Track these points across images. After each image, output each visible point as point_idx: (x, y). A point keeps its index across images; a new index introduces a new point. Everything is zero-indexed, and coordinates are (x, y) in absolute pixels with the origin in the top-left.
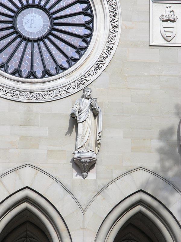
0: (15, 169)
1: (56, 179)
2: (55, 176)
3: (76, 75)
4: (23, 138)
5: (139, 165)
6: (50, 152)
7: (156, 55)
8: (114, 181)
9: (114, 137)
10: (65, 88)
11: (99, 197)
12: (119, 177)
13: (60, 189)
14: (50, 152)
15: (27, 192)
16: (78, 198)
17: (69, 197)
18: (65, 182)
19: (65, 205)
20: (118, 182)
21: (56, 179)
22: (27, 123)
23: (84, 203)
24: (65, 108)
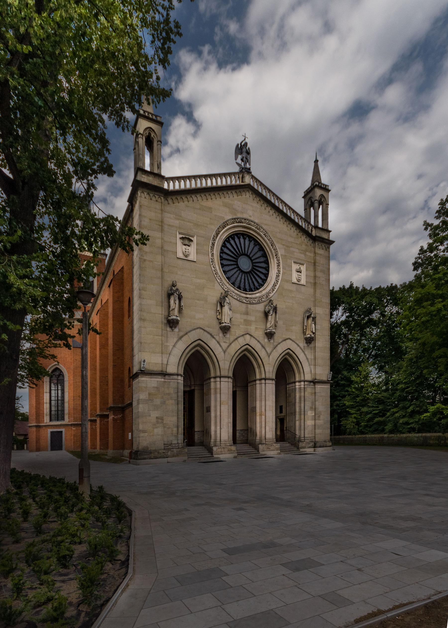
0: (243, 335)
1: (259, 341)
3: (264, 292)
4: (245, 320)
5: (288, 337)
7: (294, 288)
8: (279, 343)
9: (280, 323)
10: (261, 297)
11: (274, 351)
12: (281, 342)
13: (260, 346)
14: (256, 328)
15: (247, 346)
17: (263, 350)
18: (262, 342)
19: (263, 354)
20: (281, 344)
21: (259, 341)
22: (247, 313)
23: (269, 352)
24: (261, 307)
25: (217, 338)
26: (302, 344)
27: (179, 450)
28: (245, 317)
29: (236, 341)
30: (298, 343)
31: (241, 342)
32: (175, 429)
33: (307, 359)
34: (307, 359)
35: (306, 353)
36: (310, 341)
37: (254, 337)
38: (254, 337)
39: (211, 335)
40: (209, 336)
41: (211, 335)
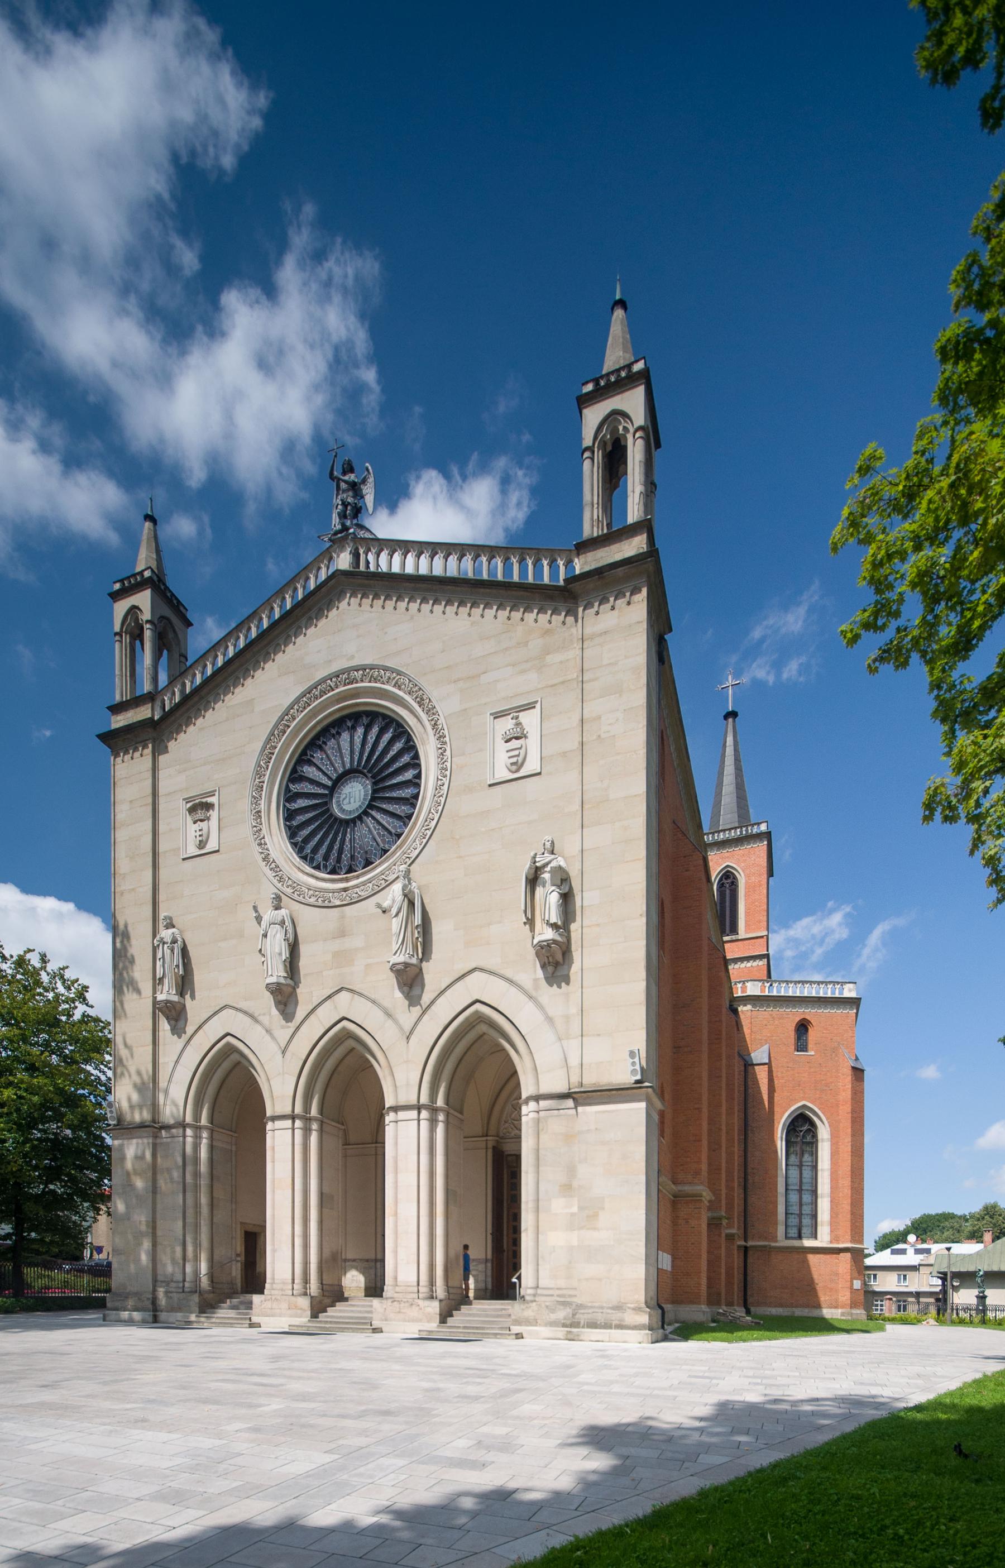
0: (329, 997)
1: (374, 1002)
2: (373, 997)
4: (336, 954)
5: (474, 966)
6: (368, 966)
13: (379, 1014)
14: (368, 966)
16: (401, 1021)
17: (390, 1022)
18: (386, 1003)
20: (447, 993)
25: (265, 1020)
26: (532, 973)
27: (182, 1295)
28: (336, 945)
29: (312, 1017)
30: (508, 973)
31: (326, 1016)
32: (179, 1250)
33: (550, 1020)
34: (550, 1020)
35: (544, 1000)
36: (556, 961)
37: (361, 994)
38: (361, 994)
39: (251, 1016)
40: (248, 1020)
41: (251, 1016)
